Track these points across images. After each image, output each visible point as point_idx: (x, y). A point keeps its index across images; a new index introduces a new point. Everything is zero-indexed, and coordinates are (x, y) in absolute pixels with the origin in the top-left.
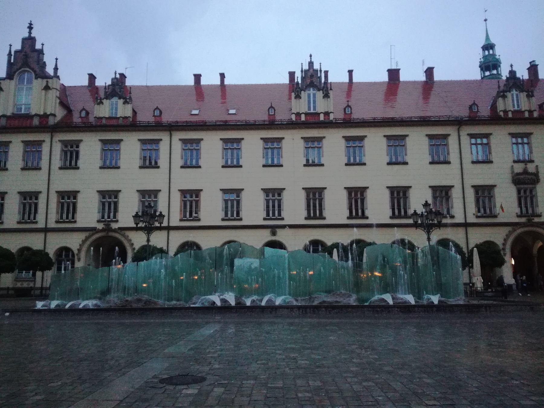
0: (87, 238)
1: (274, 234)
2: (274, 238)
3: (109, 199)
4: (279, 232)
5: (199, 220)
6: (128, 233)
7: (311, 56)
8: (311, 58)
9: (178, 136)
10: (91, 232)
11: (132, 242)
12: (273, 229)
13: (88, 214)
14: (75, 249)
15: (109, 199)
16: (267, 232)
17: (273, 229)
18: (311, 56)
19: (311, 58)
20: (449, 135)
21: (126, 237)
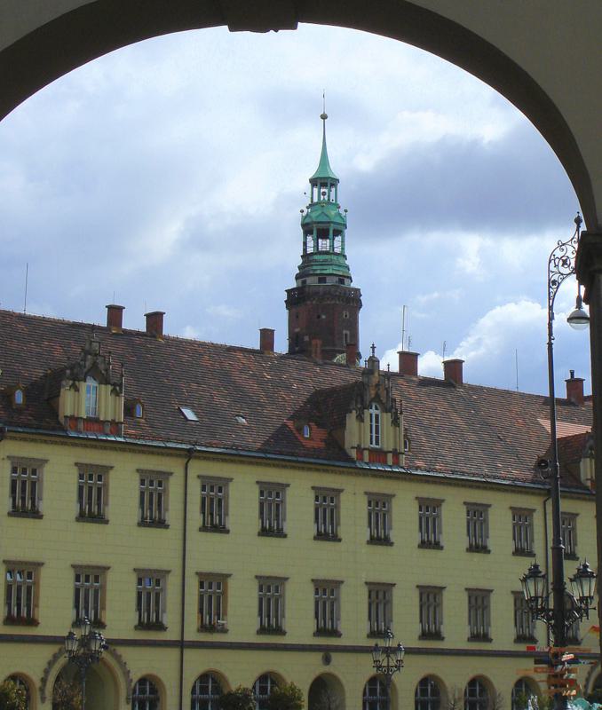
0: (56, 657)
1: (327, 660)
2: (326, 669)
3: (89, 580)
4: (335, 656)
5: (224, 631)
6: (121, 650)
7: (373, 348)
8: (373, 352)
9: (197, 468)
10: (54, 649)
11: (128, 667)
12: (327, 653)
13: (55, 610)
14: (35, 675)
15: (89, 580)
16: (317, 658)
17: (327, 653)
18: (373, 348)
19: (373, 352)
20: (534, 510)
21: (118, 658)
